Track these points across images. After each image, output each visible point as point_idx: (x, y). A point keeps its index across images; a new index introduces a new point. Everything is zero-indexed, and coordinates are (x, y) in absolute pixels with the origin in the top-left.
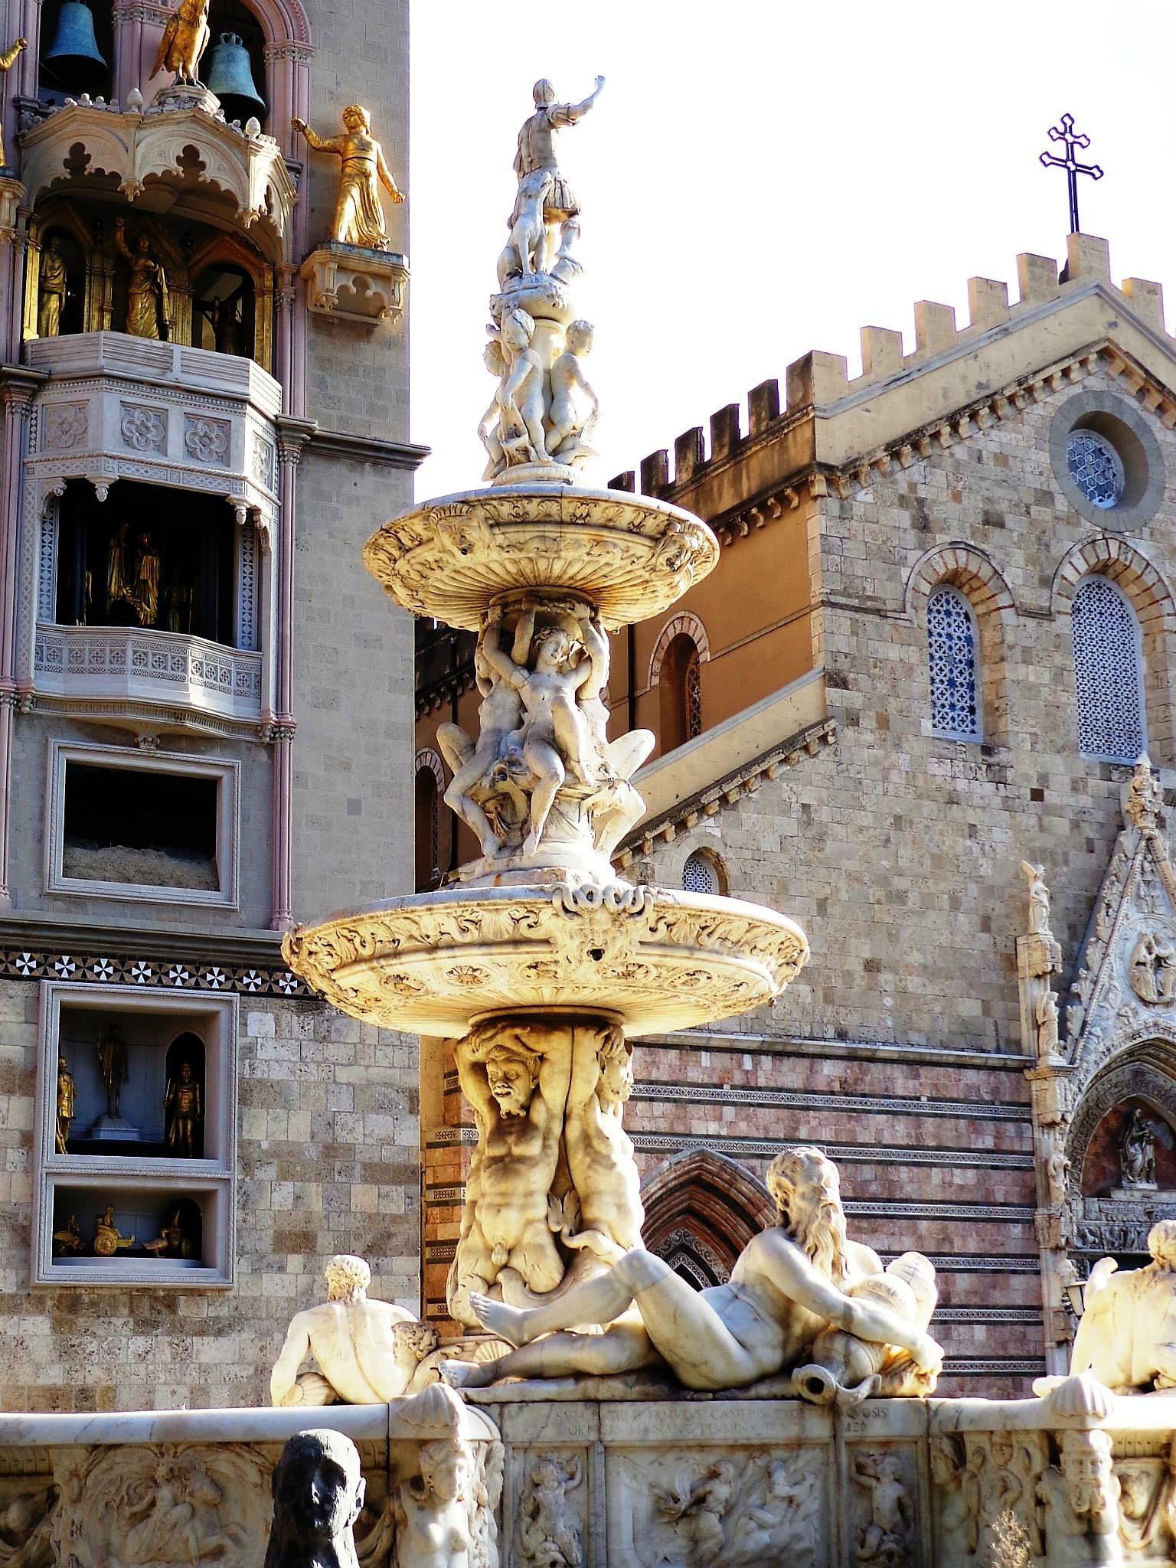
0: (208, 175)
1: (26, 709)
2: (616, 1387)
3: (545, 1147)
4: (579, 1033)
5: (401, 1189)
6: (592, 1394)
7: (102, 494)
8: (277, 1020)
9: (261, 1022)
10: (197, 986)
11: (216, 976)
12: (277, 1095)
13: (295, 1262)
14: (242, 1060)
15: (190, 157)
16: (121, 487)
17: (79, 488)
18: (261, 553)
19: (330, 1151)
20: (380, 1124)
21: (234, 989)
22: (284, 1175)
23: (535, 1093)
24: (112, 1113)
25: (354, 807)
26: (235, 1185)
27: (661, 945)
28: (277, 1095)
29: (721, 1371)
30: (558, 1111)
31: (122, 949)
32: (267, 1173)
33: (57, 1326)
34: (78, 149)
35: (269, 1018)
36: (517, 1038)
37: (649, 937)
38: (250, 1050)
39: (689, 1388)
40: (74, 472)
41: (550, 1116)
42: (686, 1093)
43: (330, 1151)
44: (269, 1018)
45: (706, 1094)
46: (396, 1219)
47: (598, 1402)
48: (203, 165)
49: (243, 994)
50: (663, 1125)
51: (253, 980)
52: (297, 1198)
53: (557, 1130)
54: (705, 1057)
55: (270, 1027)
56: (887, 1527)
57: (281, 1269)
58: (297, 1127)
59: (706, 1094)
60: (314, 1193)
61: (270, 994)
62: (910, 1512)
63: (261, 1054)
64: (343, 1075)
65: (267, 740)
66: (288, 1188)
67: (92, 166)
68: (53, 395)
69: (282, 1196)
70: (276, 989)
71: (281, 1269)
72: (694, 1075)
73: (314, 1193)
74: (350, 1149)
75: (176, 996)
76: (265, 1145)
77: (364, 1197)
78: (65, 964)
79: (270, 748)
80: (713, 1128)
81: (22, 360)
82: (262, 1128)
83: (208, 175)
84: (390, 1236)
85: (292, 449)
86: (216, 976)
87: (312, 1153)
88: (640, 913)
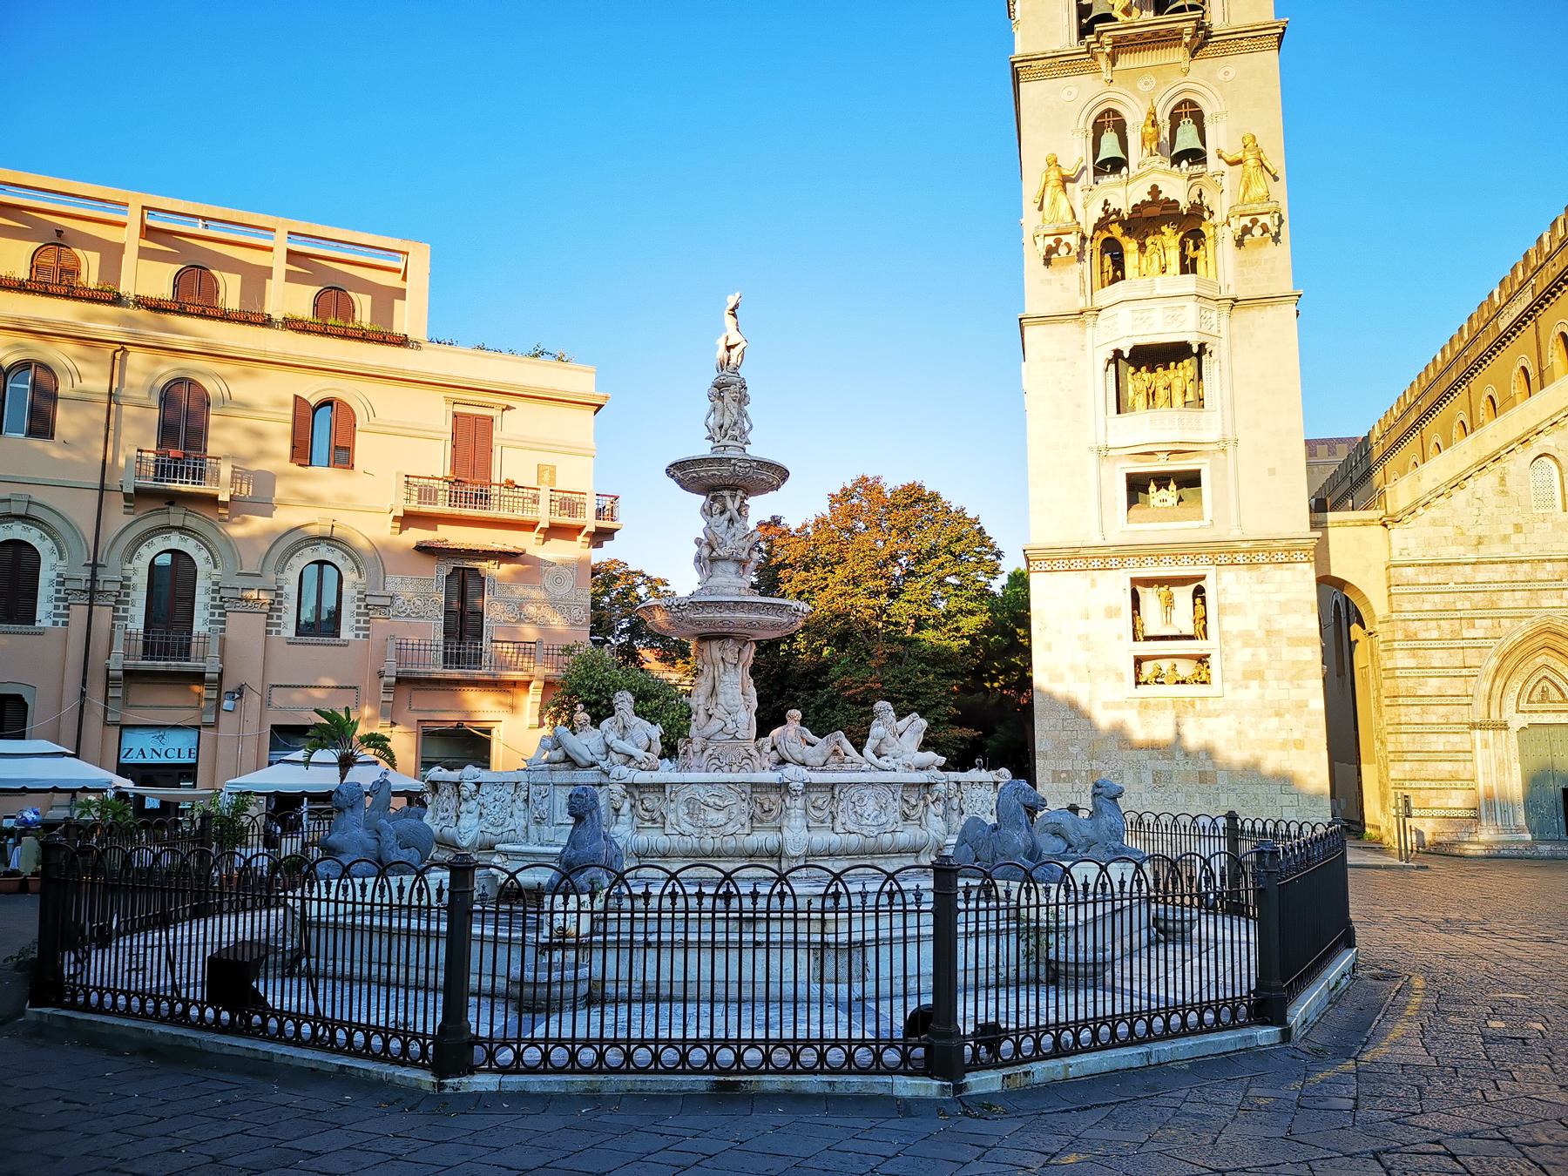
1: (1104, 452)
7: (1126, 355)
9: (1229, 576)
12: (1237, 609)
13: (1254, 684)
15: (1155, 191)
17: (1118, 354)
19: (1269, 633)
22: (1246, 645)
25: (1272, 472)
28: (1237, 609)
29: (584, 763)
31: (1155, 552)
34: (1155, 187)
42: (1537, 586)
45: (1552, 585)
46: (1306, 663)
50: (1522, 603)
51: (1223, 559)
54: (1548, 566)
59: (1552, 585)
60: (1263, 654)
71: (1247, 687)
72: (1543, 576)
73: (1263, 654)
74: (1279, 633)
77: (1288, 654)
80: (1557, 603)
82: (1232, 624)
87: (1259, 634)
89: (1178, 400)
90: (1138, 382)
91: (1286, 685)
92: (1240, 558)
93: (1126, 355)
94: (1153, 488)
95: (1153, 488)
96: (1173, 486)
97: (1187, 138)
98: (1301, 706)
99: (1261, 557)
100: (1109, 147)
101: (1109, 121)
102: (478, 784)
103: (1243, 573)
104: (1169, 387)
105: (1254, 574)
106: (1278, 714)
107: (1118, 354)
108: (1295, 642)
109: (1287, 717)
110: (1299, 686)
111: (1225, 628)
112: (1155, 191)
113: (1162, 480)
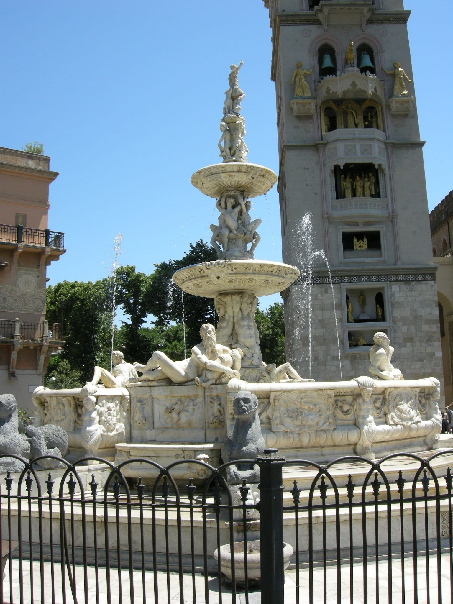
0: (358, 87)
2: (155, 383)
3: (228, 324)
4: (233, 296)
5: (435, 325)
6: (150, 385)
7: (342, 168)
8: (399, 287)
9: (395, 288)
10: (378, 281)
11: (383, 278)
13: (408, 344)
14: (391, 297)
15: (354, 84)
16: (347, 165)
17: (337, 167)
18: (384, 175)
19: (416, 317)
20: (428, 310)
21: (388, 281)
23: (226, 312)
24: (363, 312)
25: (415, 233)
26: (392, 327)
27: (235, 274)
30: (232, 316)
32: (400, 324)
33: (352, 362)
35: (397, 286)
36: (220, 299)
37: (231, 272)
38: (393, 295)
39: (173, 382)
40: (335, 164)
41: (230, 316)
43: (416, 317)
44: (397, 286)
47: (151, 386)
48: (357, 85)
49: (390, 281)
51: (392, 278)
52: (408, 329)
53: (232, 320)
55: (398, 289)
56: (216, 415)
57: (405, 346)
58: (407, 313)
60: (413, 328)
61: (397, 281)
62: (222, 412)
63: (396, 295)
64: (417, 299)
65: (392, 219)
66: (405, 327)
67: (331, 92)
68: (330, 146)
69: (404, 329)
70: (398, 280)
71: (405, 346)
75: (374, 285)
76: (399, 317)
77: (425, 328)
78: (346, 279)
79: (392, 221)
81: (322, 140)
82: (397, 313)
83: (358, 87)
84: (433, 337)
85: (389, 148)
86: (383, 278)
88: (224, 266)
89: (368, 193)
90: (346, 184)
91: (424, 344)
92: (401, 278)
93: (342, 168)
94: (355, 240)
95: (355, 240)
96: (365, 240)
97: (367, 61)
98: (432, 355)
99: (411, 278)
100: (327, 62)
101: (326, 50)
102: (97, 397)
103: (404, 287)
104: (363, 187)
105: (408, 286)
106: (421, 360)
107: (337, 167)
108: (429, 322)
109: (425, 361)
110: (430, 345)
111: (394, 315)
112: (354, 84)
113: (360, 236)
